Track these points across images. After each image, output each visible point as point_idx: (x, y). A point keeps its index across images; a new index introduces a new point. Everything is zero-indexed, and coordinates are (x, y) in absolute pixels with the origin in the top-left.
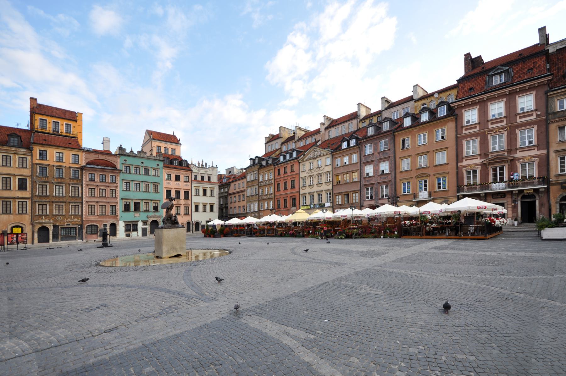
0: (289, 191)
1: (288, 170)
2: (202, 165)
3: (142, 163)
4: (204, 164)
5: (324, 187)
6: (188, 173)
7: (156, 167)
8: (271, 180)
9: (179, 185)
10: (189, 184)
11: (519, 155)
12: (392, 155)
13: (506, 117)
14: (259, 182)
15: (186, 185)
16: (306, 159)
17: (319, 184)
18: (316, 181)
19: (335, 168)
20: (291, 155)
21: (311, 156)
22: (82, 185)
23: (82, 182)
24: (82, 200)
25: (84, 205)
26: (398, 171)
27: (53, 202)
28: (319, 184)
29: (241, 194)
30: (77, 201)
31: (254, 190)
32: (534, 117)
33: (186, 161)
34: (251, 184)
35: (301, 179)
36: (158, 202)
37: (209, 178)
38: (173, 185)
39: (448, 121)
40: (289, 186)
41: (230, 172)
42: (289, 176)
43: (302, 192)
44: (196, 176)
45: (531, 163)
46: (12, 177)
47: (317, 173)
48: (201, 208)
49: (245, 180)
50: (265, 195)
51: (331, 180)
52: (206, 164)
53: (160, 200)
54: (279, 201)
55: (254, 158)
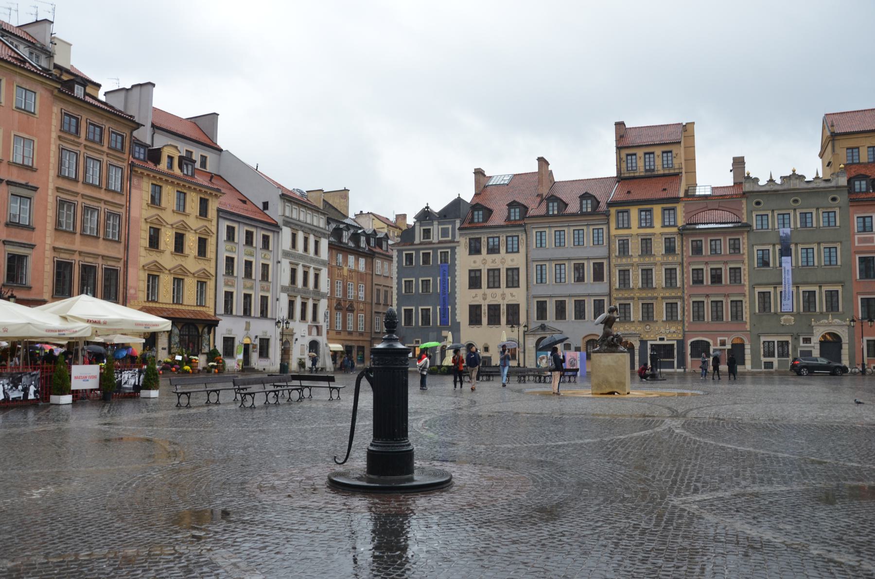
46: (586, 263)
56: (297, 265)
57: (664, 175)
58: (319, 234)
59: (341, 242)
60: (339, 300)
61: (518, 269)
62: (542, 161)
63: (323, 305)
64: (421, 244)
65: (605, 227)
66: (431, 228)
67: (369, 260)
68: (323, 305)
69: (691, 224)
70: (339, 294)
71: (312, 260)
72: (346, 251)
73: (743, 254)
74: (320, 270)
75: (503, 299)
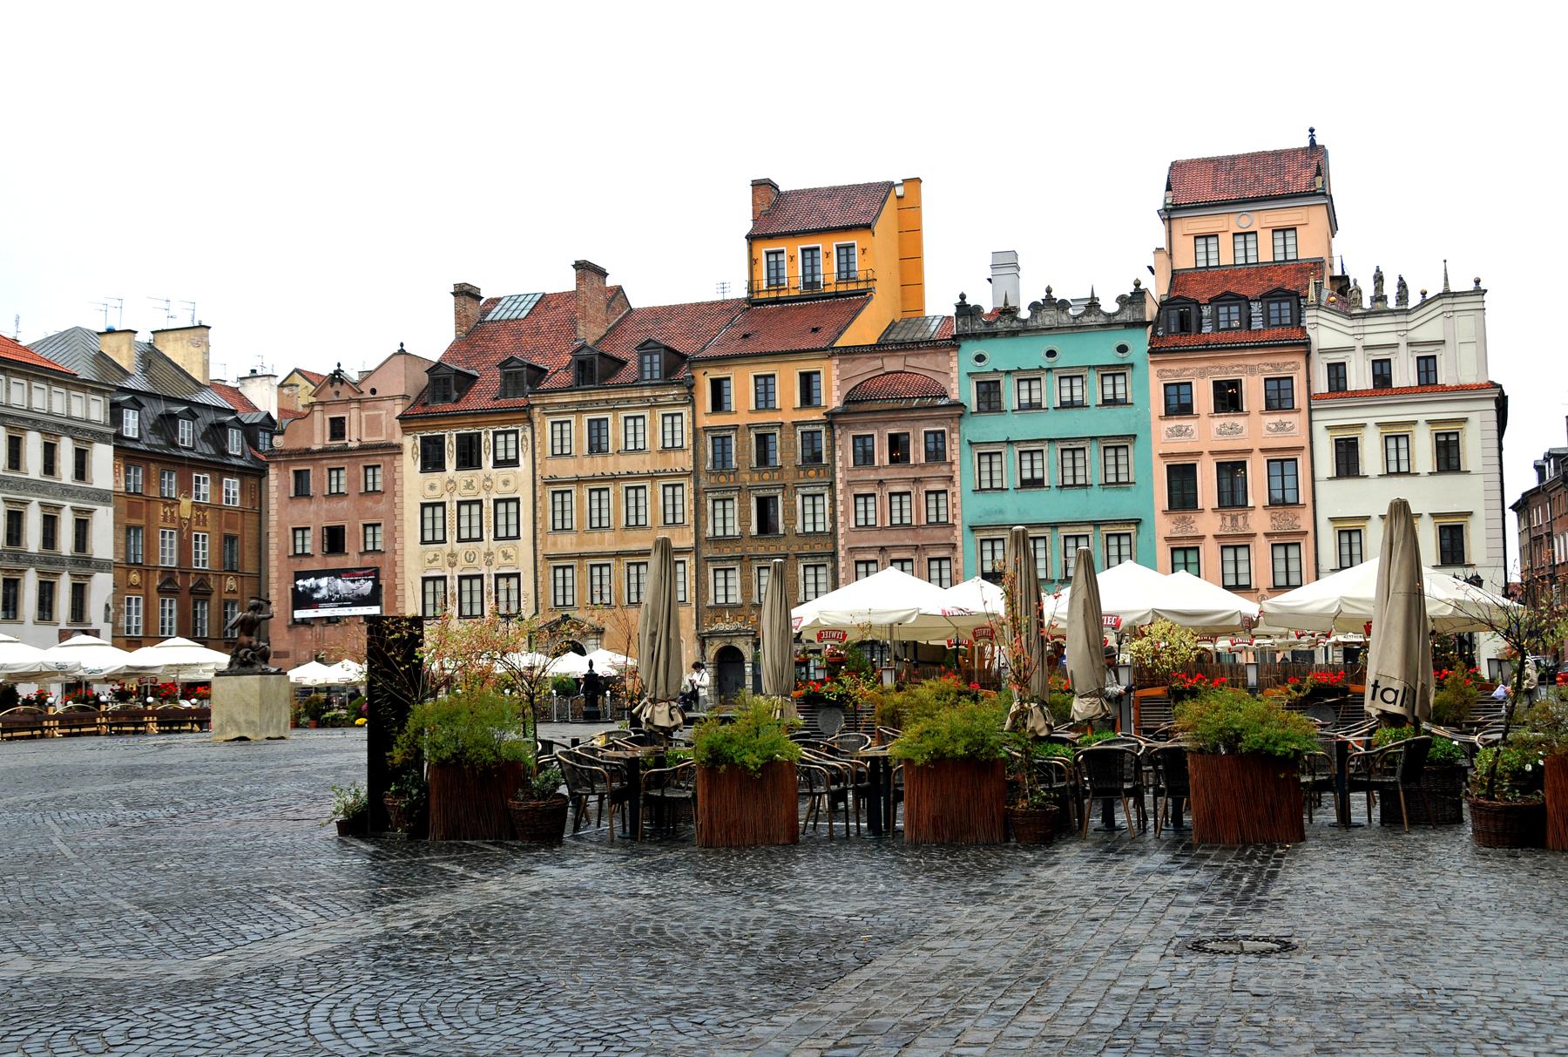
2: (1379, 298)
3: (1051, 353)
4: (1390, 290)
6: (1288, 364)
7: (1113, 358)
9: (1235, 430)
10: (1296, 421)
15: (1280, 427)
22: (832, 486)
23: (833, 475)
24: (835, 545)
25: (842, 564)
27: (751, 558)
30: (818, 549)
36: (1132, 529)
37: (1427, 366)
38: (1206, 434)
44: (1337, 373)
52: (1402, 285)
53: (1138, 522)
56: (25, 503)
57: (837, 295)
58: (84, 435)
59: (175, 446)
60: (168, 573)
61: (517, 500)
62: (586, 269)
63: (101, 587)
64: (323, 451)
65: (686, 411)
66: (346, 415)
67: (253, 482)
68: (101, 587)
69: (854, 402)
70: (170, 559)
71: (66, 491)
72: (186, 466)
73: (952, 463)
74: (90, 511)
75: (489, 563)
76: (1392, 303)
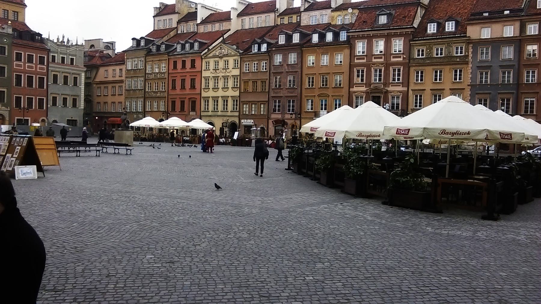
0: (188, 91)
1: (188, 65)
5: (231, 93)
8: (164, 73)
11: (391, 88)
12: (299, 70)
13: (384, 55)
14: (146, 74)
16: (211, 55)
17: (225, 88)
18: (221, 84)
19: (244, 73)
20: (192, 46)
21: (217, 54)
26: (303, 87)
28: (225, 88)
29: (117, 85)
31: (139, 84)
32: (401, 59)
33: (40, 35)
34: (133, 73)
35: (203, 79)
37: (72, 60)
39: (345, 48)
40: (188, 84)
41: (92, 46)
42: (188, 72)
43: (204, 94)
44: (54, 57)
45: (398, 97)
47: (223, 75)
48: (60, 102)
49: (123, 67)
50: (154, 92)
51: (238, 86)
52: (68, 40)
54: (174, 103)
55: (138, 37)
76: (66, 44)
